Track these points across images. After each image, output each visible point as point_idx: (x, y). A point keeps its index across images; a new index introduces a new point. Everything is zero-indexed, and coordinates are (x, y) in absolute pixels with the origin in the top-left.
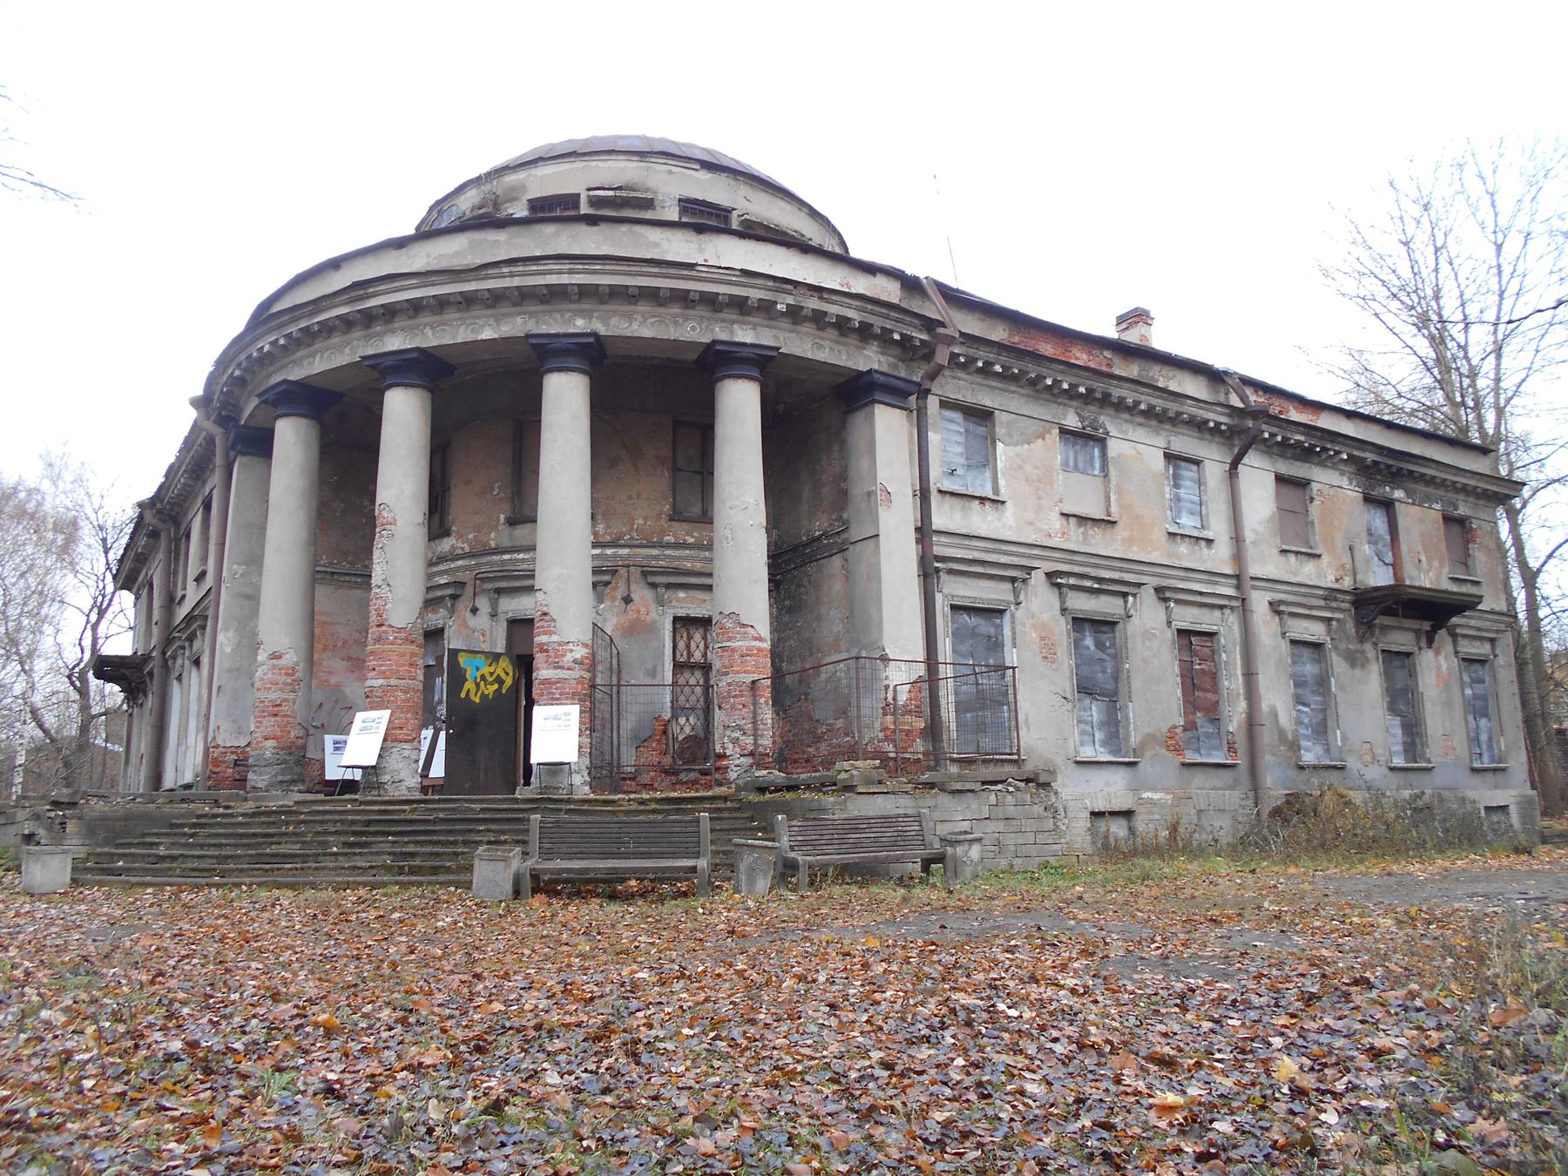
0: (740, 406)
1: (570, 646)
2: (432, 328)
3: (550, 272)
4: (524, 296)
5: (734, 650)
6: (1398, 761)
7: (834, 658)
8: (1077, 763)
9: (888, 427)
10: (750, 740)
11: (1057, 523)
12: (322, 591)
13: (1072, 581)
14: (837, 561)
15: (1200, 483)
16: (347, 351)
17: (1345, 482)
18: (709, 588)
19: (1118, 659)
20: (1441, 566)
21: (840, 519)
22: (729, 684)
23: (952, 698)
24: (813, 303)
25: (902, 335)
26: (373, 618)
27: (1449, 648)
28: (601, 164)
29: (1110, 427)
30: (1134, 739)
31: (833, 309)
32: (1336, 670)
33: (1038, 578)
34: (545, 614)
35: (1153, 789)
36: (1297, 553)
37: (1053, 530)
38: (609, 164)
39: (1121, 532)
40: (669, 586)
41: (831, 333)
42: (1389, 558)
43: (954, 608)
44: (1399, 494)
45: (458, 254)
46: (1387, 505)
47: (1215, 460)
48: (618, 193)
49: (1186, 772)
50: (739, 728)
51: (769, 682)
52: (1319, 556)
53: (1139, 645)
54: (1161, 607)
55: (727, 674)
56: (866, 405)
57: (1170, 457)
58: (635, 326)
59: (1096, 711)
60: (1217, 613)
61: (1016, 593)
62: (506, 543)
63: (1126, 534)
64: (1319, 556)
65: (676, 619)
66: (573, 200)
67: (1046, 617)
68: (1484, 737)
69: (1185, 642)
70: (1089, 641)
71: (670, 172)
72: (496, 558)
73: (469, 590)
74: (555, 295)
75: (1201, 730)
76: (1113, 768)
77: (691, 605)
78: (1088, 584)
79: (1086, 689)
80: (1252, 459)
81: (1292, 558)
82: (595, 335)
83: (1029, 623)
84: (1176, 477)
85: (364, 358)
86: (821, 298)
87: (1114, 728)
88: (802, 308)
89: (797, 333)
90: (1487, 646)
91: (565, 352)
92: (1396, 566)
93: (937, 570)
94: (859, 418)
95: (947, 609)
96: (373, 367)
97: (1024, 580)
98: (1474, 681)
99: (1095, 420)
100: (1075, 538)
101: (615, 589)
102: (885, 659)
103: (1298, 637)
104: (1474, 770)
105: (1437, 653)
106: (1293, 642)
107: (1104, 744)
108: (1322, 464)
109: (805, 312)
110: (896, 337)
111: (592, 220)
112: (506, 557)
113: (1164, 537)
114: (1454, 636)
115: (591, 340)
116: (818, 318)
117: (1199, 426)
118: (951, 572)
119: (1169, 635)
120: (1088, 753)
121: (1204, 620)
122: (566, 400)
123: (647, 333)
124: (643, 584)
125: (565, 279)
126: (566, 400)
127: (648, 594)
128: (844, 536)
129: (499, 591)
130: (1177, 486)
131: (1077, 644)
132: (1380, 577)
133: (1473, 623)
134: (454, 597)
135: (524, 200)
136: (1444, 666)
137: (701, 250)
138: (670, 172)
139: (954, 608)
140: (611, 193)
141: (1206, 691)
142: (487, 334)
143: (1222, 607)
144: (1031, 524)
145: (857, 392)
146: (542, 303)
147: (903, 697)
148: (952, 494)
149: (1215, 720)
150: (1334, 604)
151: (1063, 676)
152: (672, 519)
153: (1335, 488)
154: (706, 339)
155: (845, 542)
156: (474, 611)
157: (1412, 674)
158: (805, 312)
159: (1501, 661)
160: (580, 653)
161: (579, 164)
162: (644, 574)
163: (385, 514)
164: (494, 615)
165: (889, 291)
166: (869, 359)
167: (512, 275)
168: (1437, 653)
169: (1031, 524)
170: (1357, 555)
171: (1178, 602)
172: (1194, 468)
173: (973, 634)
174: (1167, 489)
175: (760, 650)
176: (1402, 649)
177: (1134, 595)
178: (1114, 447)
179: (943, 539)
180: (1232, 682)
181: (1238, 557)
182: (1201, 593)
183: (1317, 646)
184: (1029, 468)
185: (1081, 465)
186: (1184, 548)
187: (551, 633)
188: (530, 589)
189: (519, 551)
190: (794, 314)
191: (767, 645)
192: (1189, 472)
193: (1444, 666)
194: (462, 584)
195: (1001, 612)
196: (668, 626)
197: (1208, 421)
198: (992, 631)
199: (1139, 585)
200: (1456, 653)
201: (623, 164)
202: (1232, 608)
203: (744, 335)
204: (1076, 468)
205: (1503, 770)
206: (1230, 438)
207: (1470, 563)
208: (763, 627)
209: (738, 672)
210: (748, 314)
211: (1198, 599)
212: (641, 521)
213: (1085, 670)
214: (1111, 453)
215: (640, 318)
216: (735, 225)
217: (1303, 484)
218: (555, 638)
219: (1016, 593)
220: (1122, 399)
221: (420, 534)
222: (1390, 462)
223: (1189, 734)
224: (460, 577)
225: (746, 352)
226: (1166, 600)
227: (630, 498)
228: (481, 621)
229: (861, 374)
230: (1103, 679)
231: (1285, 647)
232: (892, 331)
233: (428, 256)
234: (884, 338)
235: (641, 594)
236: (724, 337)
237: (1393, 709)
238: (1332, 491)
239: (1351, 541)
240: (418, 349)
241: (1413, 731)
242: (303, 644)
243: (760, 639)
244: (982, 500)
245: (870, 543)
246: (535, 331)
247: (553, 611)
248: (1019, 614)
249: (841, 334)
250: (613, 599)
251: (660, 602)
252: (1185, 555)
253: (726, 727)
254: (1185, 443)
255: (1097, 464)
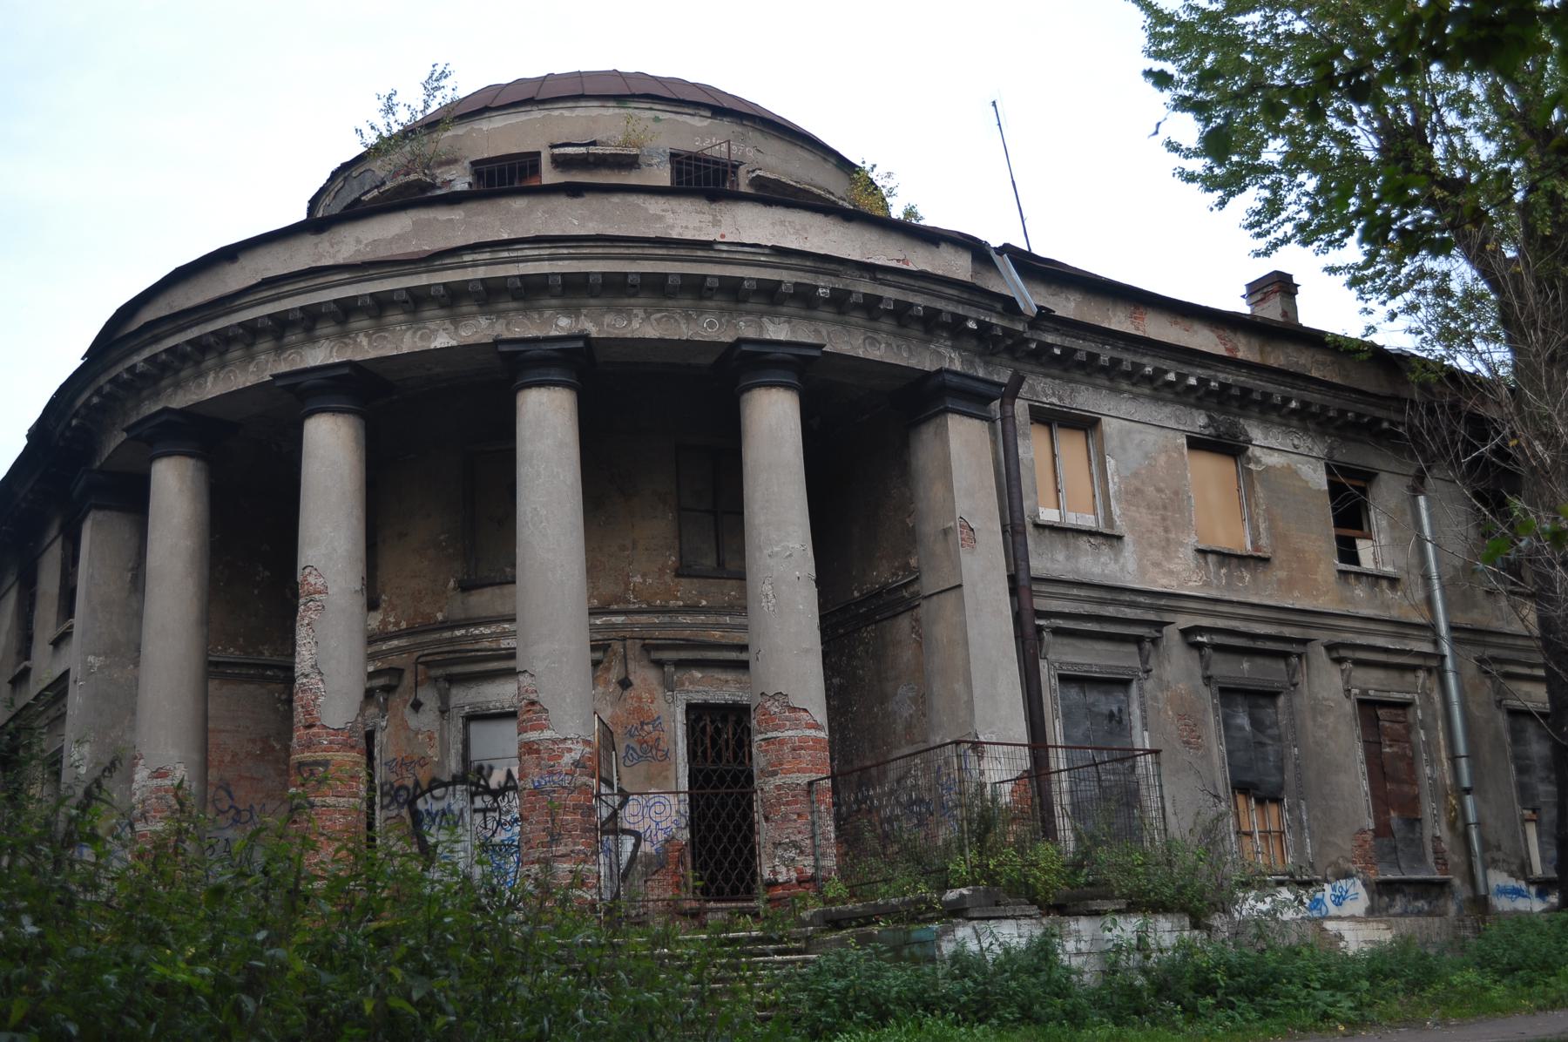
0: (774, 422)
1: (569, 744)
2: (367, 335)
3: (526, 260)
4: (490, 295)
5: (782, 742)
7: (906, 751)
9: (963, 443)
10: (809, 861)
12: (213, 685)
14: (904, 622)
16: (252, 368)
18: (744, 666)
21: (906, 567)
22: (778, 788)
23: (1066, 799)
24: (864, 287)
25: (978, 322)
26: (299, 716)
28: (566, 113)
31: (889, 293)
34: (533, 703)
37: (1179, 573)
38: (578, 112)
40: (681, 664)
41: (887, 324)
45: (398, 238)
48: (592, 150)
50: (795, 845)
51: (829, 783)
53: (1309, 724)
55: (774, 774)
56: (936, 415)
58: (636, 324)
62: (458, 614)
65: (691, 708)
66: (529, 162)
70: (1243, 720)
71: (657, 119)
72: (447, 635)
73: (408, 679)
74: (531, 291)
77: (719, 689)
82: (585, 337)
85: (276, 377)
86: (874, 279)
88: (850, 292)
89: (845, 324)
91: (545, 361)
94: (927, 433)
95: (1055, 682)
96: (289, 388)
101: (608, 669)
102: (977, 746)
109: (853, 299)
110: (972, 325)
111: (574, 190)
112: (458, 633)
115: (580, 344)
116: (871, 306)
118: (1057, 632)
119: (1349, 707)
122: (547, 422)
123: (651, 331)
124: (645, 662)
125: (545, 268)
126: (547, 422)
127: (652, 675)
128: (916, 587)
129: (453, 680)
134: (389, 690)
135: (466, 163)
137: (716, 223)
138: (657, 119)
140: (583, 150)
142: (442, 341)
145: (924, 399)
146: (515, 299)
147: (1006, 795)
152: (679, 574)
154: (727, 338)
155: (916, 595)
156: (417, 706)
158: (853, 299)
160: (577, 752)
161: (537, 114)
162: (647, 648)
163: (311, 579)
164: (444, 711)
165: (959, 266)
166: (947, 358)
167: (475, 264)
171: (1358, 663)
173: (1090, 712)
175: (817, 740)
177: (1300, 656)
179: (1044, 588)
182: (1386, 650)
187: (542, 728)
188: (512, 673)
189: (477, 624)
190: (840, 303)
191: (824, 735)
194: (398, 672)
196: (680, 717)
199: (1304, 642)
201: (595, 112)
203: (778, 331)
208: (820, 714)
209: (789, 771)
210: (781, 304)
212: (638, 579)
215: (641, 314)
216: (744, 187)
218: (547, 734)
220: (1267, 396)
221: (361, 600)
224: (396, 661)
225: (780, 353)
226: (1339, 661)
227: (623, 548)
228: (427, 719)
229: (927, 375)
232: (966, 318)
233: (358, 241)
234: (955, 329)
235: (644, 677)
236: (751, 333)
240: (349, 363)
242: (195, 757)
243: (816, 727)
245: (952, 595)
246: (507, 335)
247: (544, 699)
249: (901, 325)
250: (607, 683)
251: (669, 686)
253: (777, 845)
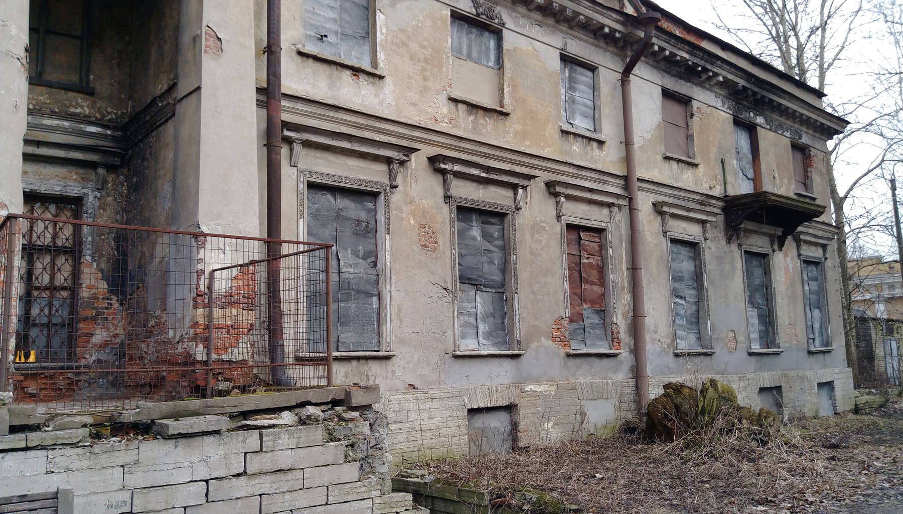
6: (756, 347)
8: (456, 357)
11: (445, 108)
13: (457, 168)
15: (595, 88)
17: (719, 104)
19: (506, 250)
20: (790, 183)
27: (795, 252)
29: (506, 18)
30: (520, 330)
32: (708, 267)
33: (418, 162)
35: (537, 381)
36: (679, 161)
37: (436, 112)
39: (513, 125)
42: (751, 174)
43: (312, 186)
44: (760, 120)
46: (751, 129)
47: (609, 67)
49: (572, 362)
52: (696, 165)
53: (528, 238)
54: (552, 201)
57: (566, 59)
59: (481, 302)
60: (605, 211)
61: (392, 175)
63: (519, 127)
64: (696, 165)
67: (426, 203)
68: (817, 326)
69: (574, 237)
70: (476, 232)
75: (587, 322)
76: (496, 361)
78: (475, 172)
79: (469, 279)
80: (641, 70)
81: (674, 165)
83: (407, 209)
84: (571, 80)
87: (502, 320)
90: (820, 251)
92: (756, 180)
93: (289, 141)
97: (402, 163)
98: (810, 279)
99: (490, 9)
100: (463, 124)
103: (678, 236)
104: (810, 353)
105: (786, 255)
106: (674, 241)
107: (489, 335)
108: (701, 85)
113: (557, 135)
114: (798, 241)
117: (595, 32)
119: (558, 228)
120: (469, 346)
121: (595, 217)
130: (571, 88)
131: (461, 234)
132: (742, 187)
133: (811, 231)
136: (791, 266)
139: (312, 186)
141: (592, 283)
143: (610, 205)
144: (414, 105)
148: (316, 58)
149: (602, 312)
150: (708, 209)
151: (444, 267)
153: (712, 109)
157: (767, 272)
159: (829, 264)
168: (786, 255)
169: (414, 105)
170: (727, 167)
171: (568, 197)
172: (589, 74)
174: (563, 91)
176: (761, 250)
177: (524, 187)
178: (508, 37)
180: (618, 275)
181: (628, 159)
182: (591, 190)
183: (692, 245)
184: (414, 46)
185: (475, 54)
186: (576, 147)
192: (584, 77)
193: (791, 266)
195: (375, 195)
197: (603, 26)
198: (363, 215)
199: (530, 177)
200: (799, 255)
202: (619, 207)
204: (469, 56)
205: (829, 352)
206: (623, 48)
207: (809, 183)
211: (588, 195)
213: (470, 261)
214: (506, 45)
217: (685, 101)
219: (392, 175)
222: (756, 90)
223: (575, 325)
226: (556, 195)
230: (492, 272)
231: (665, 244)
237: (752, 303)
238: (709, 110)
239: (721, 158)
241: (768, 320)
244: (356, 71)
248: (396, 198)
252: (576, 152)
254: (578, 47)
255: (492, 56)
